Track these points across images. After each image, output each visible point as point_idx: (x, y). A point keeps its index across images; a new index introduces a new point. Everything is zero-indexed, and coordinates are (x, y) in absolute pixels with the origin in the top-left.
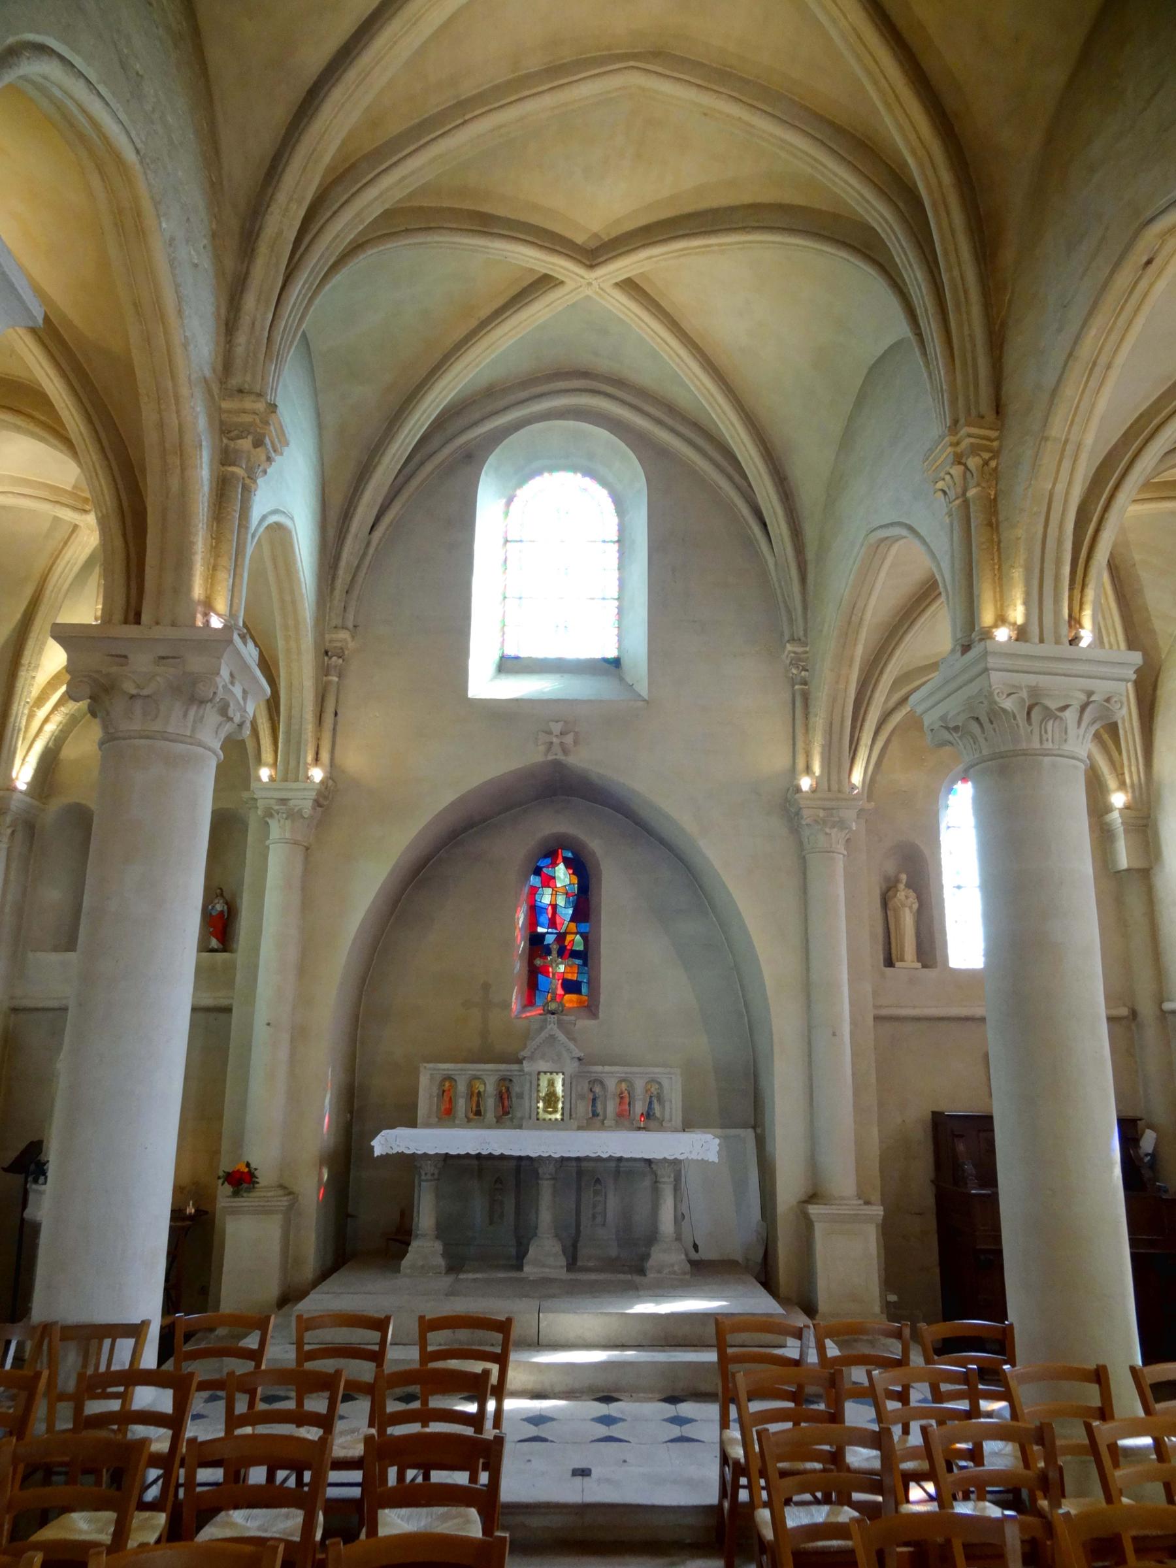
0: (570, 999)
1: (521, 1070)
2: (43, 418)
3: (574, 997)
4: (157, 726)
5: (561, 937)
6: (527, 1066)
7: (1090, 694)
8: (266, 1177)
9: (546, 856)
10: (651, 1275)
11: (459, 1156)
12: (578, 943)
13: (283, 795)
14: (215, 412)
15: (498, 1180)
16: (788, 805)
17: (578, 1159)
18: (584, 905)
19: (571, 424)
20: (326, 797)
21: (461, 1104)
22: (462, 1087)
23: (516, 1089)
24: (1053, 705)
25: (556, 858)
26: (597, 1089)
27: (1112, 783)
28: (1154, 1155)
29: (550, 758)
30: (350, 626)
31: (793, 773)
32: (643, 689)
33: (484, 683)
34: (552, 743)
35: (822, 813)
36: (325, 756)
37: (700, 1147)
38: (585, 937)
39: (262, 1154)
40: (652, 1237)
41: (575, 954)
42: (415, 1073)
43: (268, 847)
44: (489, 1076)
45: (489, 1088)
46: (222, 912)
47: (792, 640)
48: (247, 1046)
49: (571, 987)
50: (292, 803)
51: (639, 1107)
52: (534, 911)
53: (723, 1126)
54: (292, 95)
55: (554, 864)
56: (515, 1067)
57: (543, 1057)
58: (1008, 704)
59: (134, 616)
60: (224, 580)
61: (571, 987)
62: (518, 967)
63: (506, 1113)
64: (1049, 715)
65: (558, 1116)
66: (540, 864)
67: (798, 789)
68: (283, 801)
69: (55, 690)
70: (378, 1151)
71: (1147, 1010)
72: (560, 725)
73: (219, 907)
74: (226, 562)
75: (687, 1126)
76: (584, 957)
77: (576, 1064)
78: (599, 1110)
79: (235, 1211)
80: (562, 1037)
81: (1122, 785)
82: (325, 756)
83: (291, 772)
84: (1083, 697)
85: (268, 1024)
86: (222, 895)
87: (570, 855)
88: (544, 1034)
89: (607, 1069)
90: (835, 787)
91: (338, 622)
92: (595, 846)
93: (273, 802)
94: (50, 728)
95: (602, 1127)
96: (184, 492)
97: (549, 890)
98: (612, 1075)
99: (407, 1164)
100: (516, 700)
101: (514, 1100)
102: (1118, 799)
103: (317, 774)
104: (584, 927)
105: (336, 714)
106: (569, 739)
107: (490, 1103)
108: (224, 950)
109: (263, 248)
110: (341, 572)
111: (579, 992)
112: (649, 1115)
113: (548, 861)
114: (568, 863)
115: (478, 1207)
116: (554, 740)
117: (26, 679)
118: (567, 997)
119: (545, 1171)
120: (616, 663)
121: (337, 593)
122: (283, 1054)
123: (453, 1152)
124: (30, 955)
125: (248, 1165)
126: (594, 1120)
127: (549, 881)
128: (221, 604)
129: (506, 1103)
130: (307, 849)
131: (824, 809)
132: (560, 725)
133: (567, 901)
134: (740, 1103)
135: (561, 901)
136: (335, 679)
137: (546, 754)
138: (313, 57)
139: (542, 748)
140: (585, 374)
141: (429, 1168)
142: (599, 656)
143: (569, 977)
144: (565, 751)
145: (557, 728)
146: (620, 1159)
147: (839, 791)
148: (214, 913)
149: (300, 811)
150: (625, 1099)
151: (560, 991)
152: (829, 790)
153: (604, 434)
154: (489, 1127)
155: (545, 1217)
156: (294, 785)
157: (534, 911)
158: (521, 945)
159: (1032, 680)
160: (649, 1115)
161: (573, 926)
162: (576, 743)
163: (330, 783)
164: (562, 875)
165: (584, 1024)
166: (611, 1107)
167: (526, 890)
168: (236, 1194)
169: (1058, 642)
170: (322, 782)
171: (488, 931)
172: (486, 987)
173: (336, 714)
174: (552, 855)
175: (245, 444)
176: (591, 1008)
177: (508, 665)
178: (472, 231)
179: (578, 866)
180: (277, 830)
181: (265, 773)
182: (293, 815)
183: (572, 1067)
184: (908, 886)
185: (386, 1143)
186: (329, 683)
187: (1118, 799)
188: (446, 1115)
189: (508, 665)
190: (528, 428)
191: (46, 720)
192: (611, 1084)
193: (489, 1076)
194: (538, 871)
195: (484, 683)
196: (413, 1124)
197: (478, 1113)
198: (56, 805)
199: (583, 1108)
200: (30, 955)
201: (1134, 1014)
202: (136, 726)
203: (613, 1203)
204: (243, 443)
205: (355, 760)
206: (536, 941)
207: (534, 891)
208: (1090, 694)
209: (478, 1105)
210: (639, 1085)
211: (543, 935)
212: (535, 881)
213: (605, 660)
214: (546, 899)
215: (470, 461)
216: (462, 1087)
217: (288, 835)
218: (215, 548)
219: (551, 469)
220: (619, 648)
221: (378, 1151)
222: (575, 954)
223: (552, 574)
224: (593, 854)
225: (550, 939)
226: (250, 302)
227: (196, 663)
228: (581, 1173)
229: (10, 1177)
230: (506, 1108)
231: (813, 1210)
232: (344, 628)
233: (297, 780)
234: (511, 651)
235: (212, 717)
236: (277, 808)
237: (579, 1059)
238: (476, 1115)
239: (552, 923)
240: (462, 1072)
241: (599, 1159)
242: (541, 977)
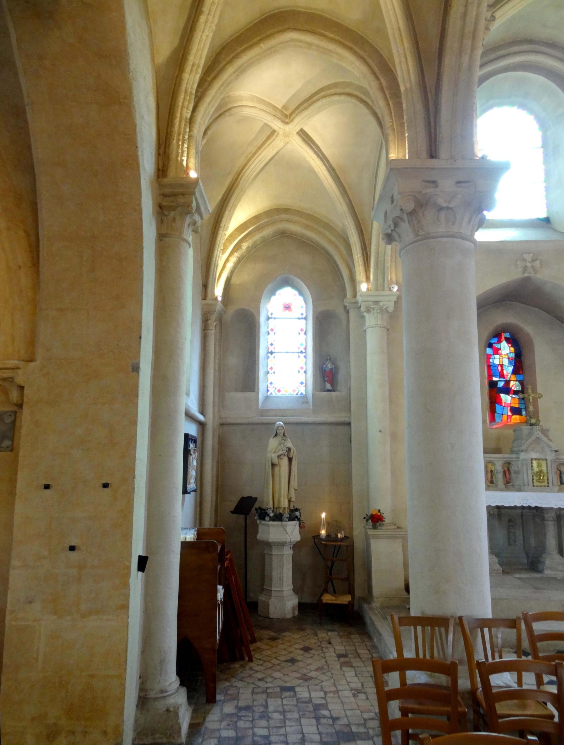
1: (518, 458)
2: (332, 36)
3: (518, 417)
4: (455, 229)
6: (522, 456)
8: (388, 517)
9: (495, 336)
11: (510, 508)
13: (377, 299)
15: (510, 521)
18: (519, 364)
19: (520, 74)
23: (513, 468)
25: (501, 338)
29: (526, 275)
34: (526, 266)
38: (522, 383)
39: (382, 504)
41: (516, 392)
43: (365, 331)
45: (499, 467)
46: (332, 369)
48: (365, 445)
49: (516, 411)
50: (381, 304)
55: (500, 341)
56: (514, 456)
57: (533, 450)
59: (433, 154)
61: (516, 411)
63: (508, 483)
65: (546, 484)
66: (492, 341)
68: (376, 303)
69: (231, 243)
72: (531, 255)
73: (330, 366)
79: (376, 537)
80: (544, 438)
85: (380, 431)
86: (330, 360)
87: (508, 335)
88: (533, 437)
93: (371, 303)
94: (230, 265)
97: (497, 357)
100: (503, 242)
101: (513, 475)
104: (521, 377)
106: (537, 264)
108: (334, 391)
111: (520, 414)
113: (496, 340)
114: (508, 340)
116: (529, 264)
117: (222, 236)
118: (514, 417)
119: (549, 516)
120: (547, 220)
123: (507, 505)
124: (227, 394)
125: (379, 511)
127: (497, 351)
129: (507, 475)
130: (388, 330)
132: (531, 255)
133: (510, 363)
135: (506, 362)
137: (524, 273)
139: (520, 270)
140: (531, 41)
143: (513, 405)
144: (535, 271)
145: (528, 257)
148: (327, 370)
149: (387, 308)
151: (510, 414)
153: (540, 79)
154: (501, 490)
161: (513, 377)
164: (506, 349)
168: (374, 527)
174: (498, 336)
180: (370, 320)
181: (364, 287)
182: (383, 311)
183: (550, 456)
190: (493, 78)
191: (227, 260)
193: (499, 461)
194: (490, 346)
197: (492, 482)
198: (231, 311)
200: (227, 394)
202: (442, 229)
206: (493, 385)
207: (489, 357)
209: (492, 478)
211: (496, 382)
212: (489, 351)
214: (497, 362)
219: (498, 105)
220: (548, 211)
222: (516, 392)
224: (528, 335)
225: (501, 384)
229: (235, 516)
233: (384, 290)
236: (372, 306)
239: (502, 375)
242: (497, 406)
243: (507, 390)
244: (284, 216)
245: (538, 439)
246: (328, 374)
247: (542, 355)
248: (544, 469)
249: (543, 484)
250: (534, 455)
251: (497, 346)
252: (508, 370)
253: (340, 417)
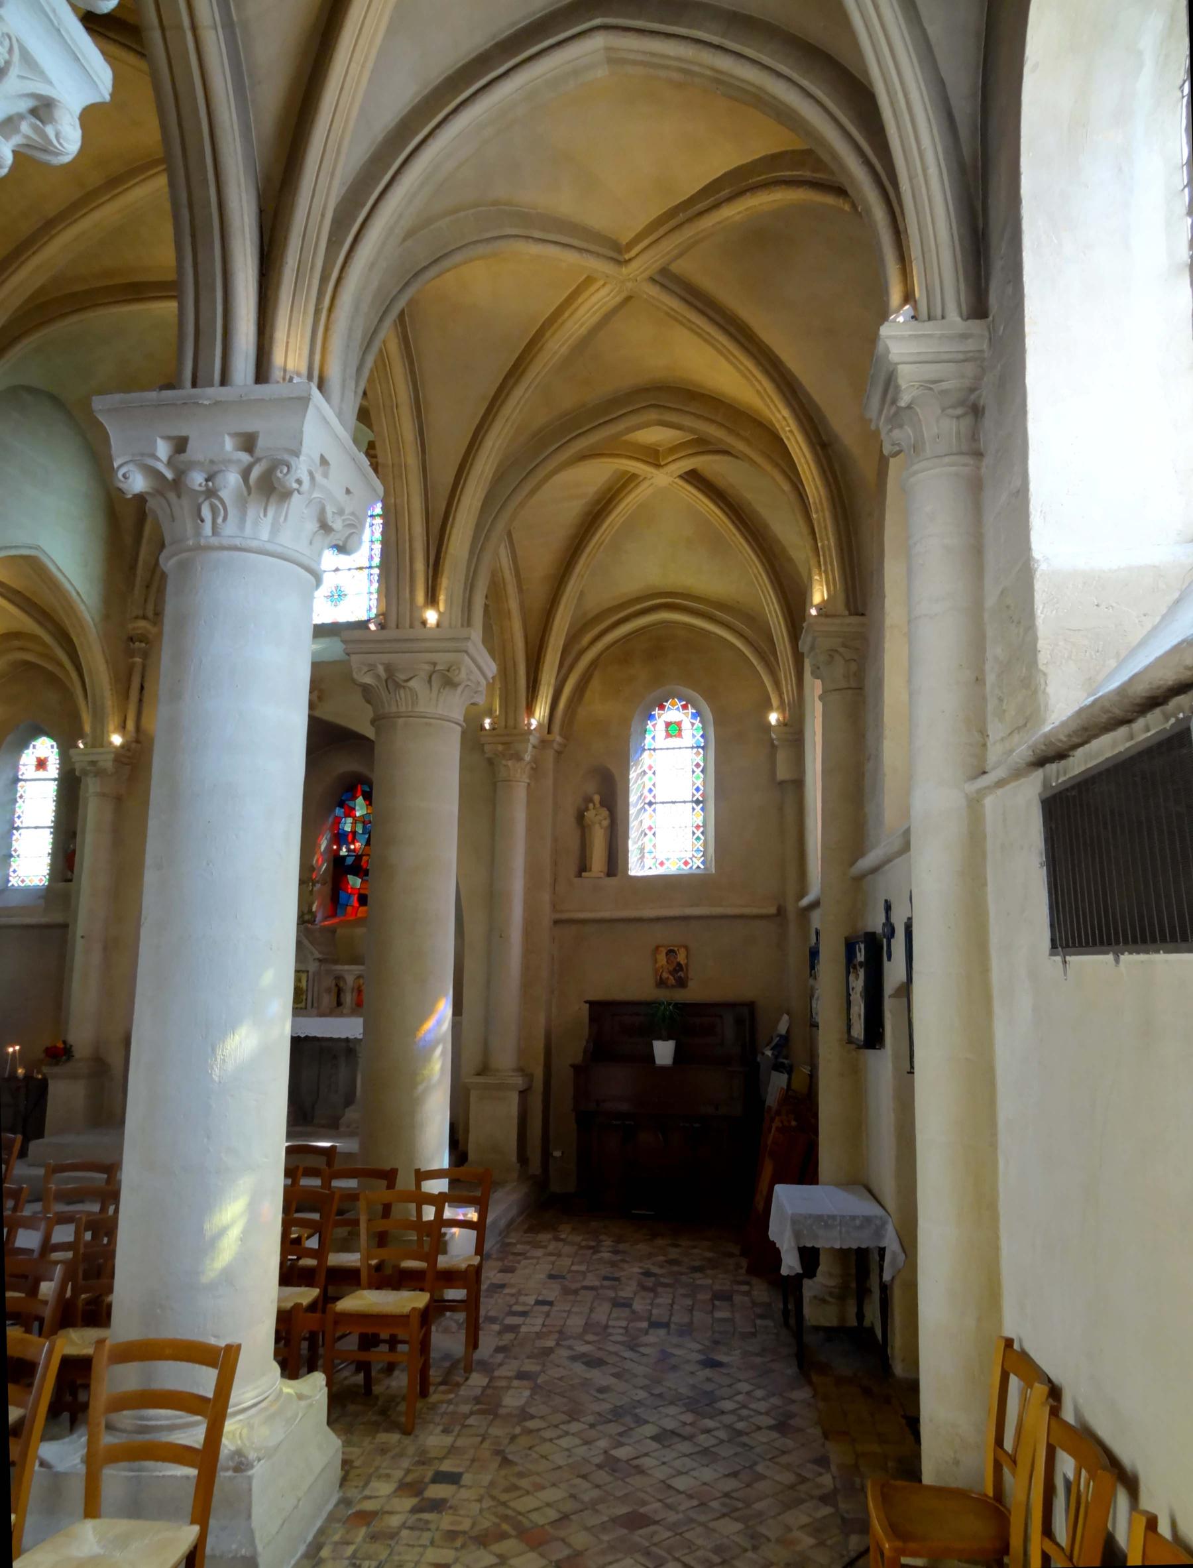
7: (435, 664)
10: (342, 1129)
24: (401, 677)
26: (341, 984)
27: (775, 702)
28: (786, 1039)
30: (150, 614)
35: (500, 748)
36: (130, 725)
55: (354, 798)
58: (368, 680)
64: (398, 686)
67: (482, 728)
68: (93, 763)
71: (791, 909)
77: (317, 964)
78: (342, 1000)
81: (782, 708)
83: (99, 740)
84: (428, 667)
89: (346, 967)
90: (511, 723)
91: (140, 613)
95: (342, 1015)
97: (350, 820)
102: (773, 718)
103: (117, 740)
105: (142, 688)
110: (140, 571)
113: (349, 795)
122: (96, 958)
125: (64, 1042)
127: (350, 812)
131: (503, 744)
136: (138, 660)
147: (515, 728)
151: (356, 904)
152: (506, 727)
156: (100, 750)
159: (386, 658)
163: (134, 745)
167: (331, 820)
169: (411, 626)
170: (122, 746)
173: (142, 688)
178: (125, 301)
182: (100, 773)
184: (602, 804)
186: (134, 664)
187: (773, 718)
192: (350, 980)
194: (341, 804)
199: (327, 1000)
201: (781, 912)
207: (338, 821)
208: (435, 664)
212: (339, 812)
217: (98, 790)
232: (145, 618)
233: (102, 746)
237: (320, 960)
242: (342, 895)
244: (16, 643)
246: (65, 857)
249: (302, 1005)
251: (351, 804)
253: (57, 918)
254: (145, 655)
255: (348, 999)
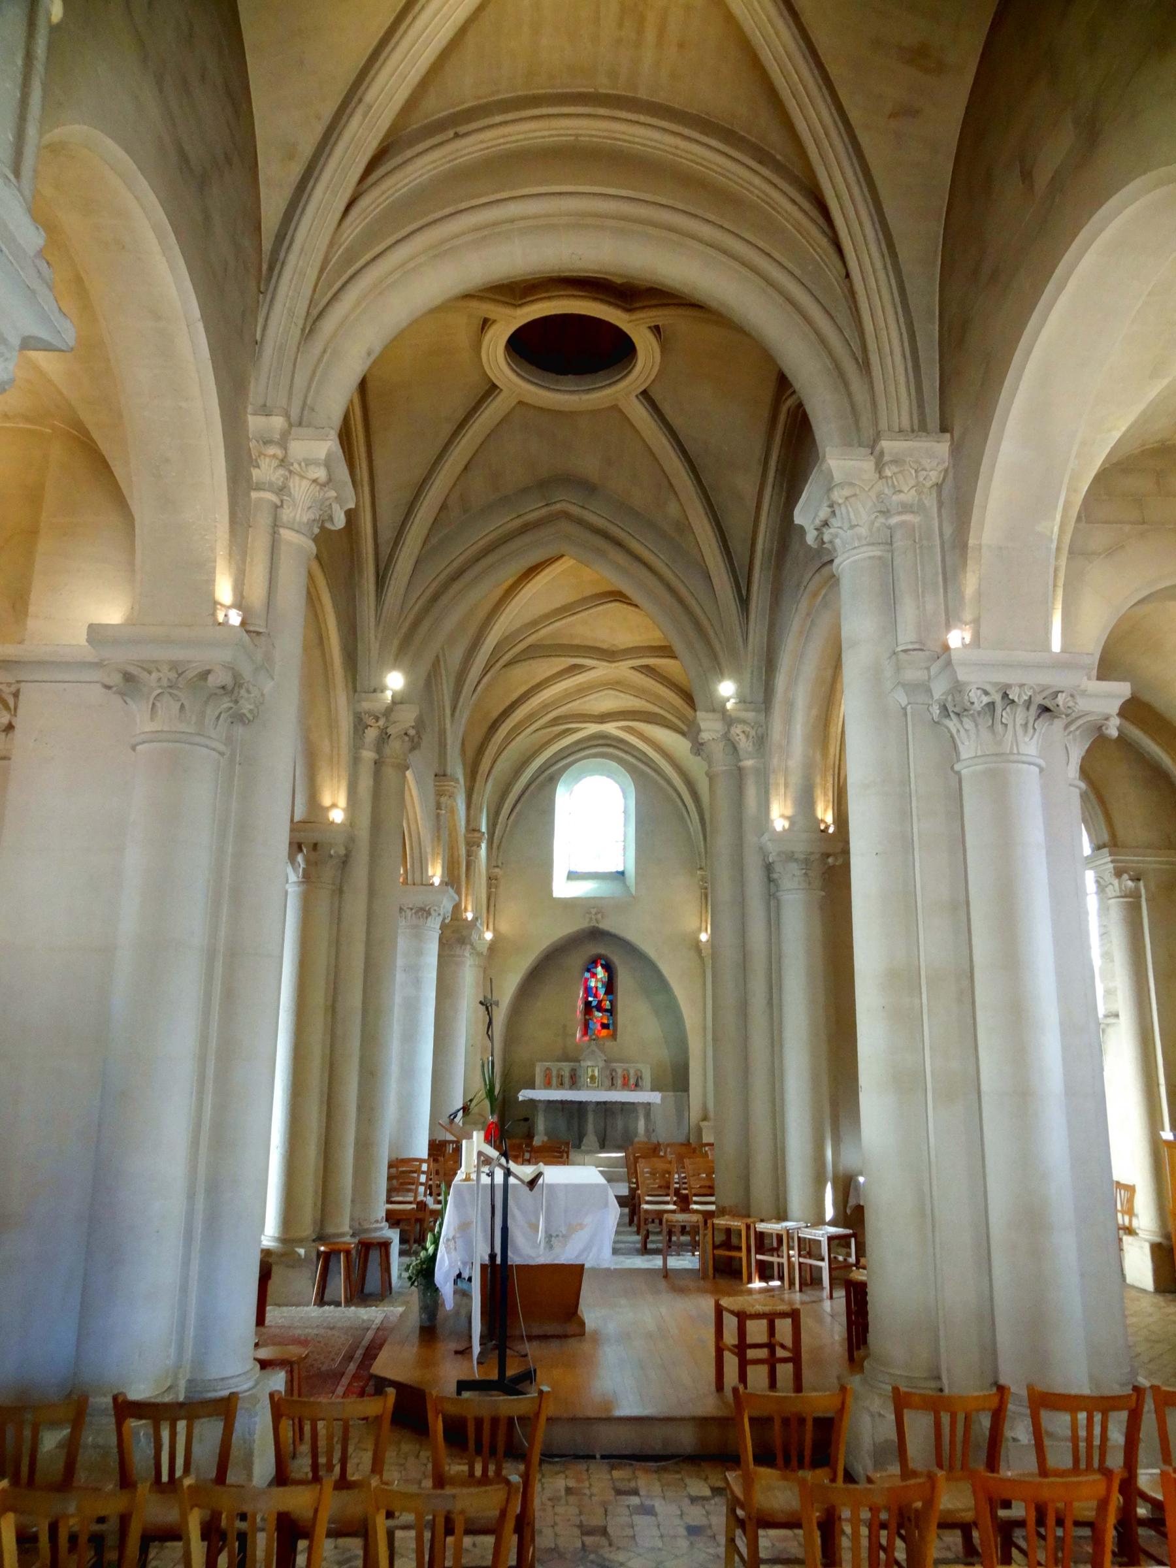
0: (604, 1032)
5: (600, 1002)
6: (583, 1064)
12: (607, 1005)
14: (466, 837)
16: (697, 946)
17: (605, 1103)
18: (610, 987)
20: (493, 947)
21: (554, 1081)
22: (554, 1073)
23: (578, 1073)
31: (700, 930)
32: (633, 890)
33: (562, 889)
36: (491, 926)
37: (655, 1097)
38: (611, 1002)
40: (636, 1134)
41: (607, 1011)
42: (533, 1066)
44: (566, 1067)
45: (566, 1074)
47: (701, 868)
49: (605, 1026)
51: (632, 1081)
52: (587, 990)
53: (674, 1091)
54: (489, 723)
60: (470, 898)
61: (605, 1026)
62: (579, 1016)
70: (521, 1098)
74: (470, 891)
75: (653, 1089)
76: (611, 1012)
82: (491, 926)
92: (616, 960)
95: (616, 1089)
96: (459, 876)
98: (619, 1068)
99: (532, 1103)
103: (489, 936)
104: (610, 997)
106: (599, 916)
107: (567, 1080)
109: (478, 777)
112: (637, 1085)
114: (603, 966)
115: (562, 1123)
119: (590, 1108)
120: (622, 873)
121: (494, 850)
126: (613, 1086)
127: (594, 975)
128: (470, 908)
134: (676, 1079)
135: (600, 985)
138: (495, 714)
141: (541, 1107)
142: (614, 870)
145: (594, 911)
146: (623, 1103)
150: (626, 1079)
153: (615, 764)
155: (590, 1127)
157: (587, 990)
158: (580, 1005)
160: (637, 1085)
162: (602, 917)
165: (609, 1044)
166: (619, 1082)
171: (565, 1003)
172: (565, 1026)
174: (594, 962)
175: (474, 848)
176: (614, 1036)
177: (572, 876)
179: (608, 968)
183: (601, 1064)
185: (524, 1095)
188: (548, 1085)
189: (572, 876)
192: (620, 1071)
193: (566, 1067)
194: (588, 970)
195: (562, 889)
196: (533, 1088)
199: (607, 1082)
203: (620, 1124)
204: (472, 845)
205: (505, 927)
206: (588, 1004)
207: (587, 980)
210: (632, 1072)
212: (587, 975)
213: (618, 872)
214: (592, 983)
215: (553, 780)
216: (554, 1073)
218: (467, 889)
221: (521, 1098)
222: (607, 1011)
223: (592, 829)
225: (594, 1004)
226: (475, 796)
227: (465, 933)
228: (606, 1109)
230: (574, 1082)
231: (704, 1124)
234: (573, 869)
235: (468, 947)
238: (561, 1085)
239: (595, 996)
240: (554, 1066)
241: (611, 1103)
243: (599, 1008)
245: (593, 1052)
247: (624, 980)
248: (596, 1074)
250: (589, 1064)
252: (602, 992)
254: (496, 887)
255: (619, 1082)
